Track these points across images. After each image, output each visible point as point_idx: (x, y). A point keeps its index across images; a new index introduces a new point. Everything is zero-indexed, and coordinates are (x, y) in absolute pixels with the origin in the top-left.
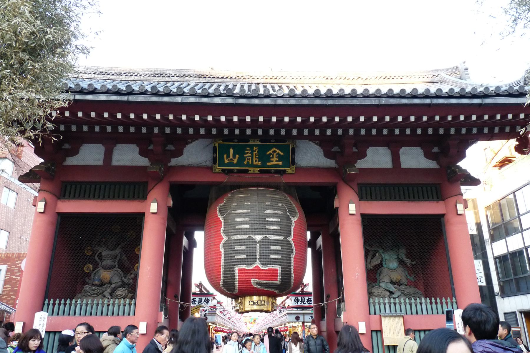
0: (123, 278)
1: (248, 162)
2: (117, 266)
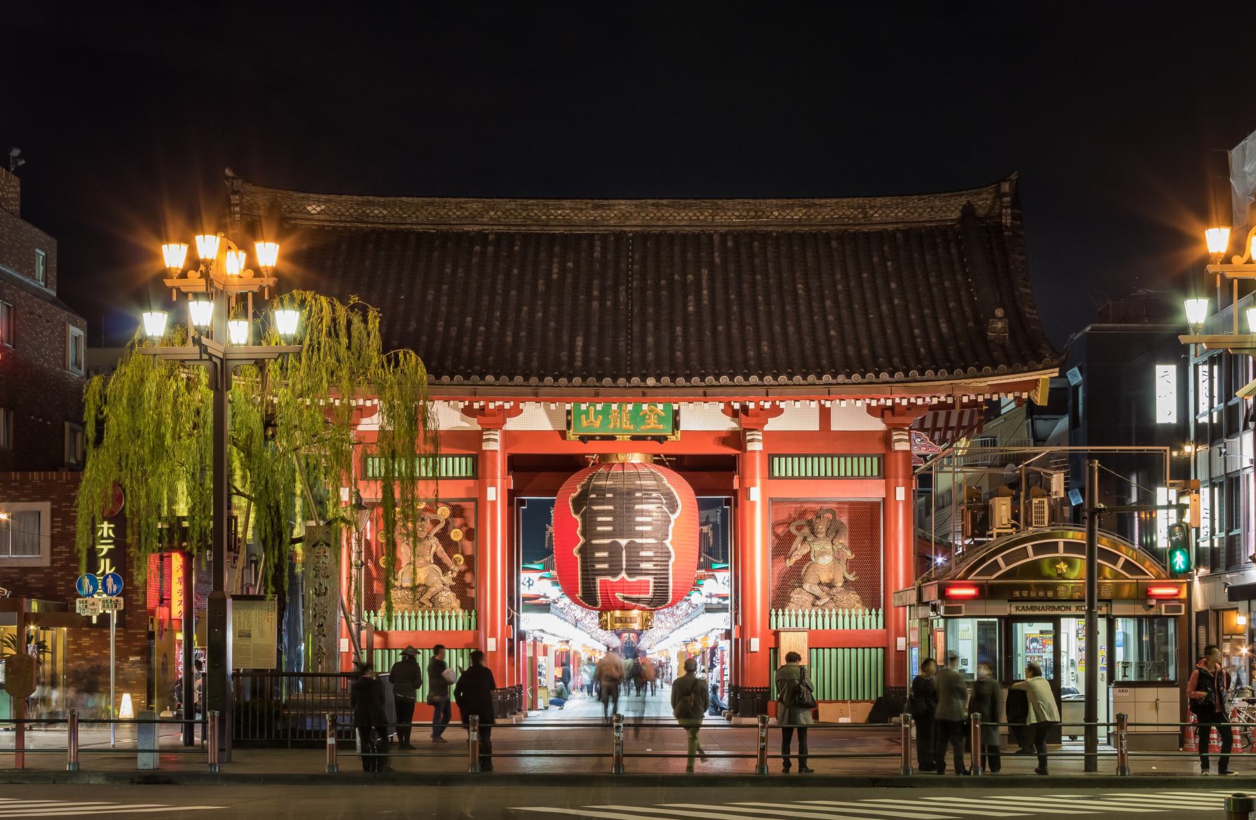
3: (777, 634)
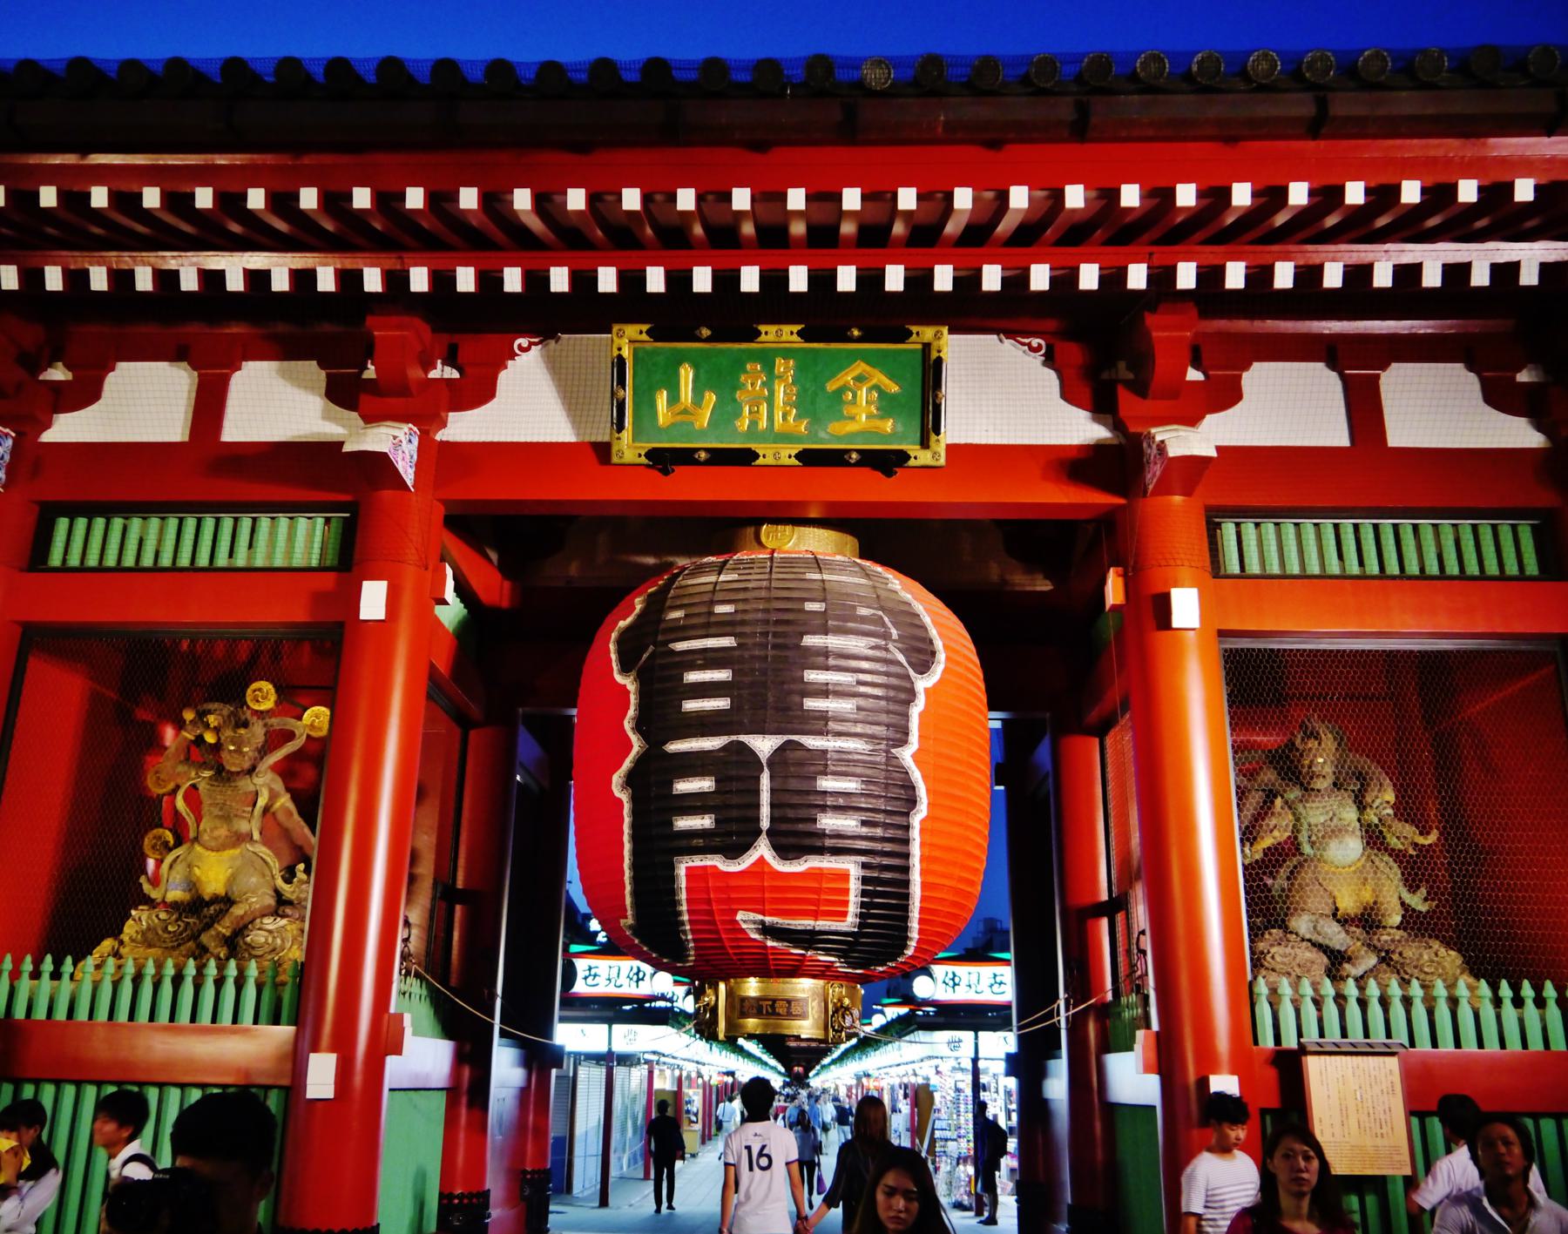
0: (280, 883)
1: (754, 423)
2: (256, 836)
3: (1289, 1065)
